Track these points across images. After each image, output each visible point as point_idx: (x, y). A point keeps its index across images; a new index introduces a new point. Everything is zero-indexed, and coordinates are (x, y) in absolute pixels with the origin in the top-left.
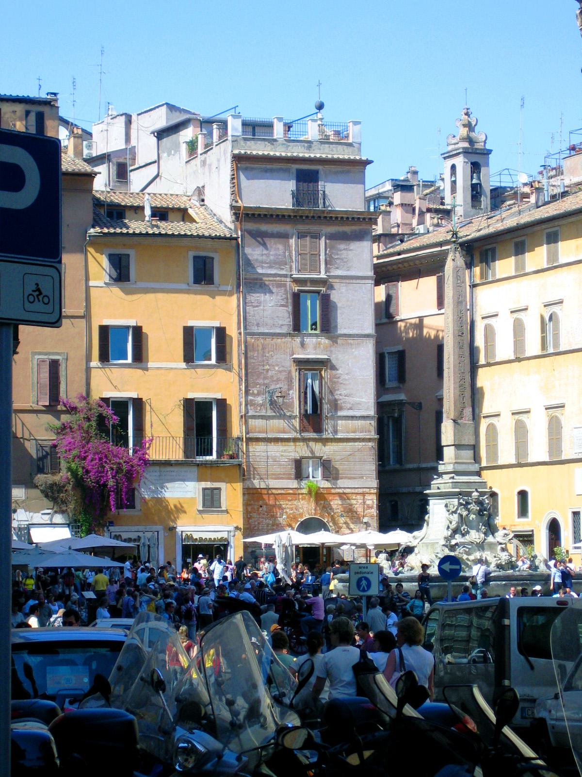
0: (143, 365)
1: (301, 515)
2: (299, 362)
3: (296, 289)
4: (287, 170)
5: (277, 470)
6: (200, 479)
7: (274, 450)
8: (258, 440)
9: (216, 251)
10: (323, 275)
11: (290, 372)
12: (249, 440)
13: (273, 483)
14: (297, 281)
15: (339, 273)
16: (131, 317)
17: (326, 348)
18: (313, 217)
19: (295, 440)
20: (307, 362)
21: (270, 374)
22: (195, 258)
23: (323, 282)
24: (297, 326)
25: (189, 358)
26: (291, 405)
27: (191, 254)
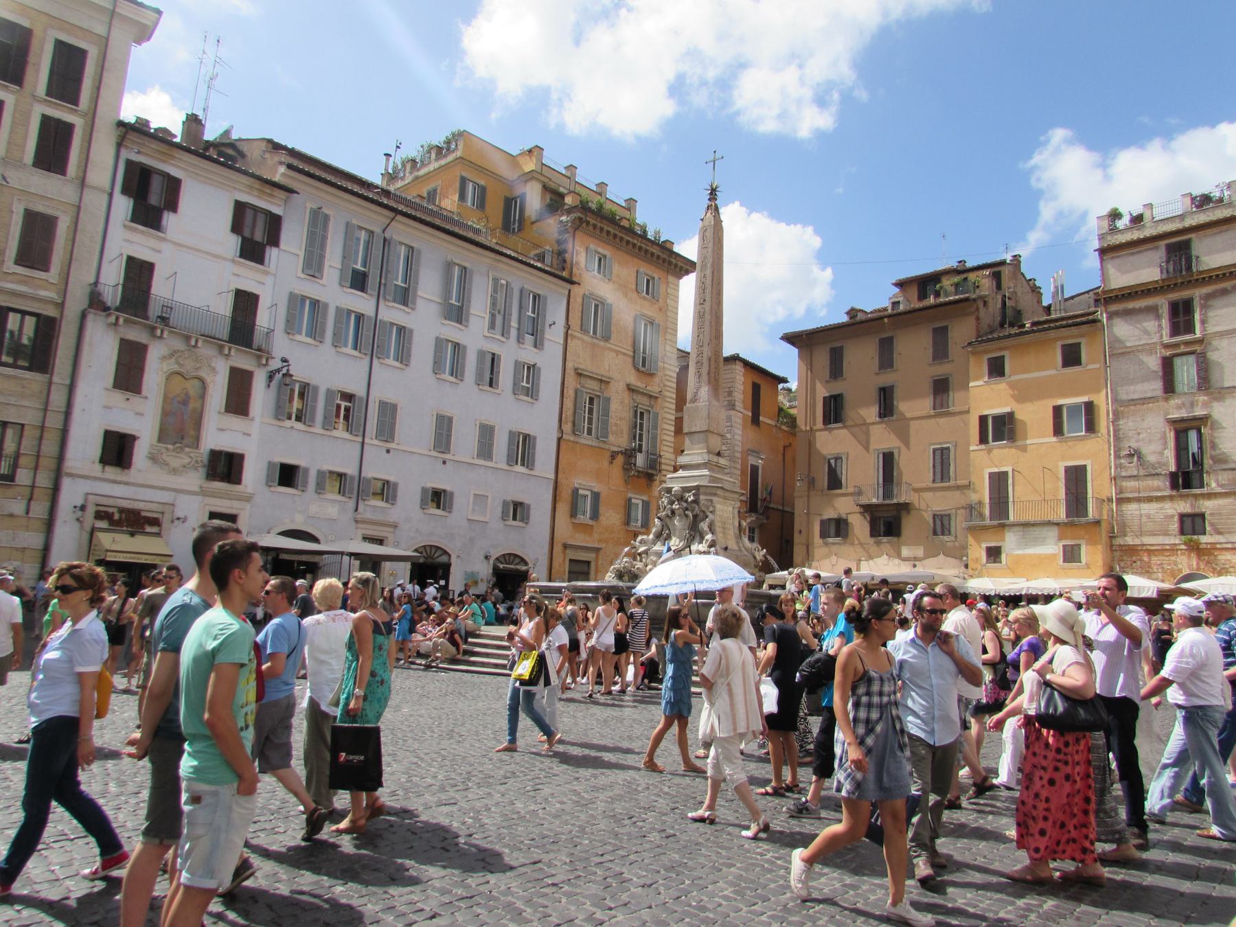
0: (1019, 443)
1: (1180, 571)
2: (1173, 422)
3: (1168, 353)
4: (1157, 248)
5: (1150, 526)
6: (1060, 538)
7: (1146, 508)
8: (1129, 500)
9: (1083, 336)
10: (1198, 334)
11: (1165, 433)
12: (1120, 501)
13: (1147, 540)
14: (1166, 346)
15: (1219, 329)
16: (1007, 405)
17: (1205, 404)
18: (1182, 283)
19: (1171, 498)
20: (1182, 420)
21: (1141, 436)
22: (1063, 346)
23: (1200, 341)
24: (1169, 387)
25: (1058, 430)
26: (1166, 464)
27: (1059, 344)
